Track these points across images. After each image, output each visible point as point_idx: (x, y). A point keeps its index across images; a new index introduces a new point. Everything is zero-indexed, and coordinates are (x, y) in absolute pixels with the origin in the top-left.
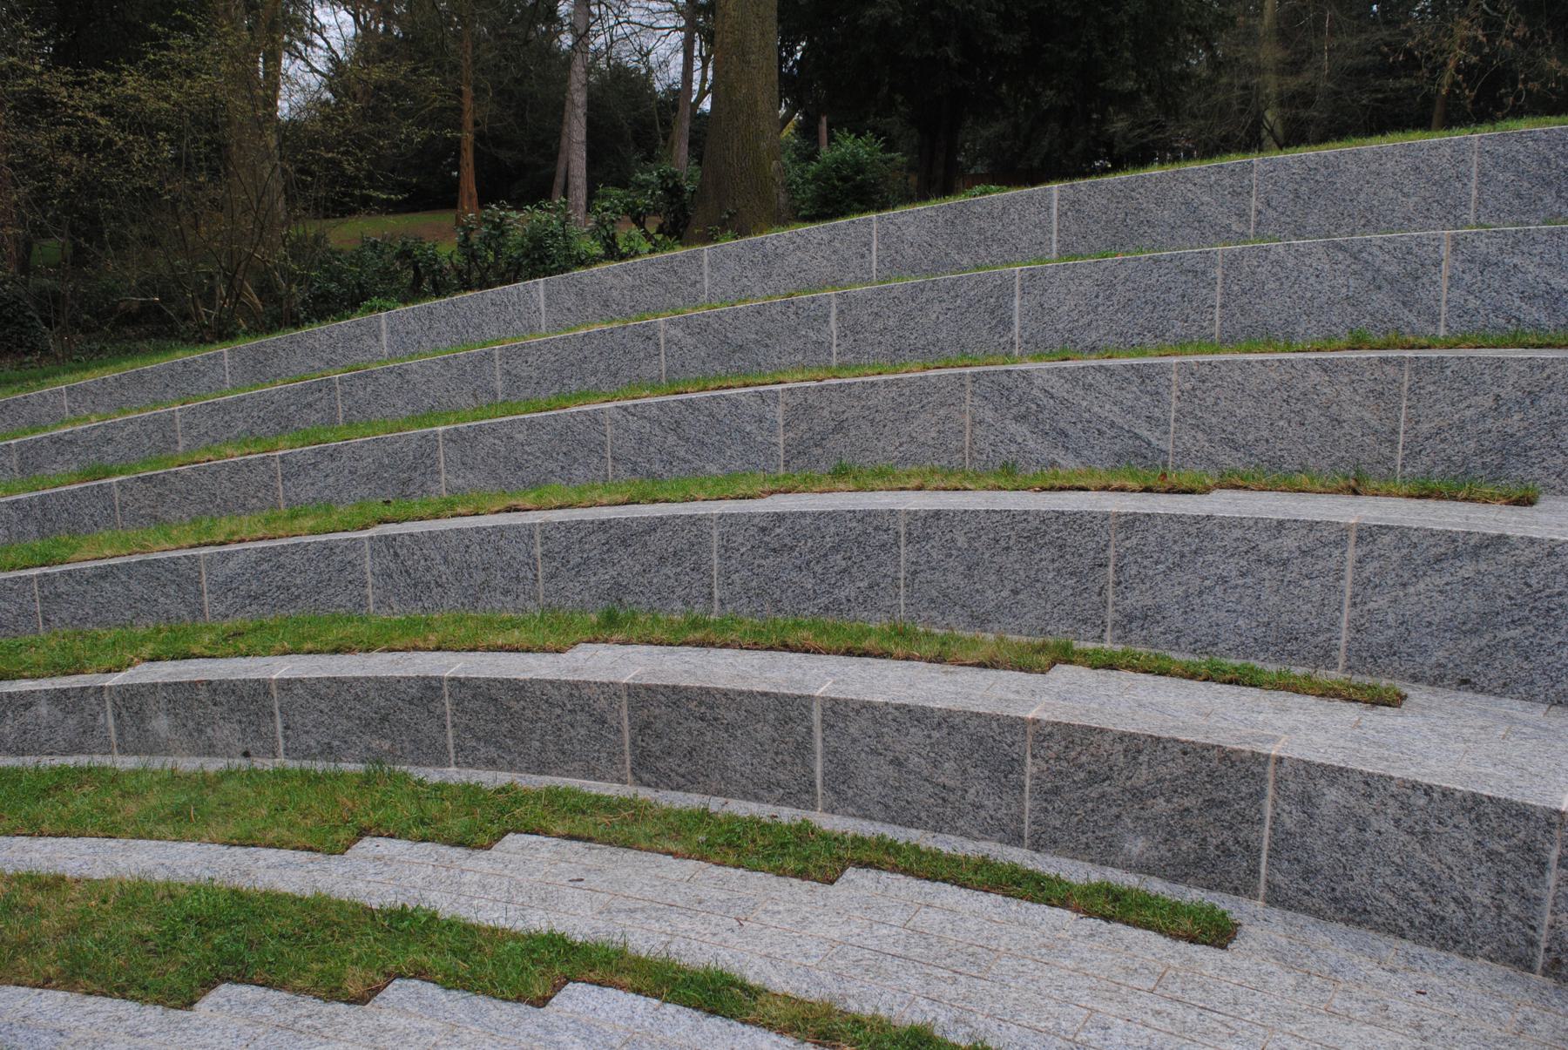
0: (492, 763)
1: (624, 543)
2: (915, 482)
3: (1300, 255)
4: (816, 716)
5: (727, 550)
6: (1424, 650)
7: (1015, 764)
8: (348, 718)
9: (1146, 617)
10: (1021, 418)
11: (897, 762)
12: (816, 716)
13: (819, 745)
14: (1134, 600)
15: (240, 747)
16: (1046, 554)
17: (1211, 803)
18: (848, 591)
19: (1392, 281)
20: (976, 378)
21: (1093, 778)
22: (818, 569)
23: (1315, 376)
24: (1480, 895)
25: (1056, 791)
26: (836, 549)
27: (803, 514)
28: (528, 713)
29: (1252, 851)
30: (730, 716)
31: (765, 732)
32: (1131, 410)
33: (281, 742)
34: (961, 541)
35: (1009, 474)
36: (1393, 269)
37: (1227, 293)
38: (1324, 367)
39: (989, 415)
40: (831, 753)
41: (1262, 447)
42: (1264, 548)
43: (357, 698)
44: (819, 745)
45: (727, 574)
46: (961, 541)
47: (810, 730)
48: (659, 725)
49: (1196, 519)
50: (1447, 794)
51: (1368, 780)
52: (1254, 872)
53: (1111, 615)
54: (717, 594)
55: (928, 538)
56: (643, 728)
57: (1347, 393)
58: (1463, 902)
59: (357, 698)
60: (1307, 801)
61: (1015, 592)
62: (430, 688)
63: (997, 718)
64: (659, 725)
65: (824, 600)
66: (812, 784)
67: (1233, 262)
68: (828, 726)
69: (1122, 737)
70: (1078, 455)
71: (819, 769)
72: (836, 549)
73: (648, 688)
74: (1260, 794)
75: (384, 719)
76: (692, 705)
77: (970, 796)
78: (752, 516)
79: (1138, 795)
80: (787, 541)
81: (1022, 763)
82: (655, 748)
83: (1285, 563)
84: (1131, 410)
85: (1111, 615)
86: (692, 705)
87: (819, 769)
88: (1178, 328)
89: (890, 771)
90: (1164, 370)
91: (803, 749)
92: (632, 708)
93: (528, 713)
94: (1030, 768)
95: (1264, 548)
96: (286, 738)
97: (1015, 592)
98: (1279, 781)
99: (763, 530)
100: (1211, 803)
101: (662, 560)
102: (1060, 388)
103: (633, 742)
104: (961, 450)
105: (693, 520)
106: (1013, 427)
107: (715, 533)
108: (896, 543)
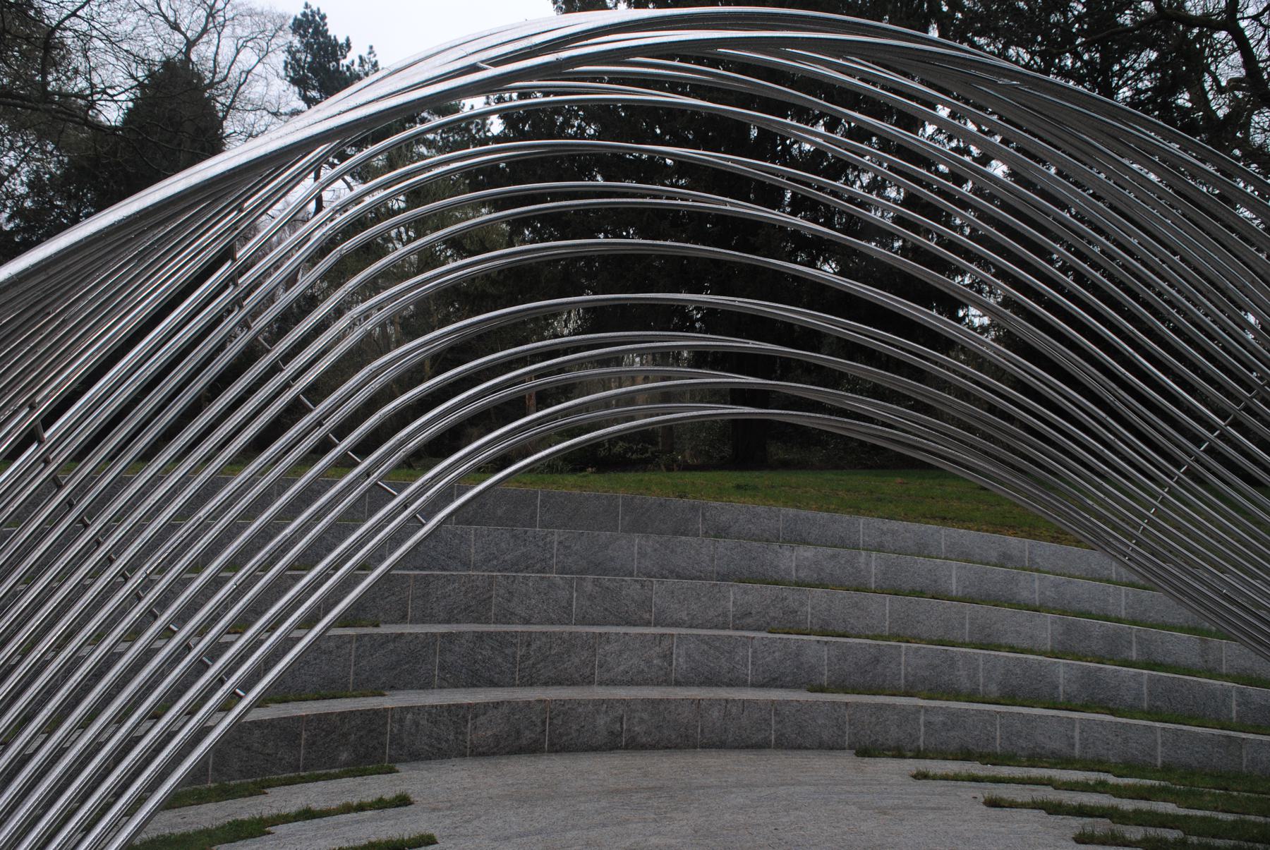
6: (378, 678)
11: (248, 749)
17: (370, 731)
24: (451, 737)
25: (314, 743)
29: (383, 745)
50: (441, 706)
51: (419, 708)
52: (384, 753)
58: (447, 741)
60: (401, 720)
63: (292, 718)
69: (340, 714)
74: (386, 723)
79: (345, 735)
81: (300, 734)
83: (331, 652)
94: (304, 735)
98: (393, 716)
100: (370, 731)
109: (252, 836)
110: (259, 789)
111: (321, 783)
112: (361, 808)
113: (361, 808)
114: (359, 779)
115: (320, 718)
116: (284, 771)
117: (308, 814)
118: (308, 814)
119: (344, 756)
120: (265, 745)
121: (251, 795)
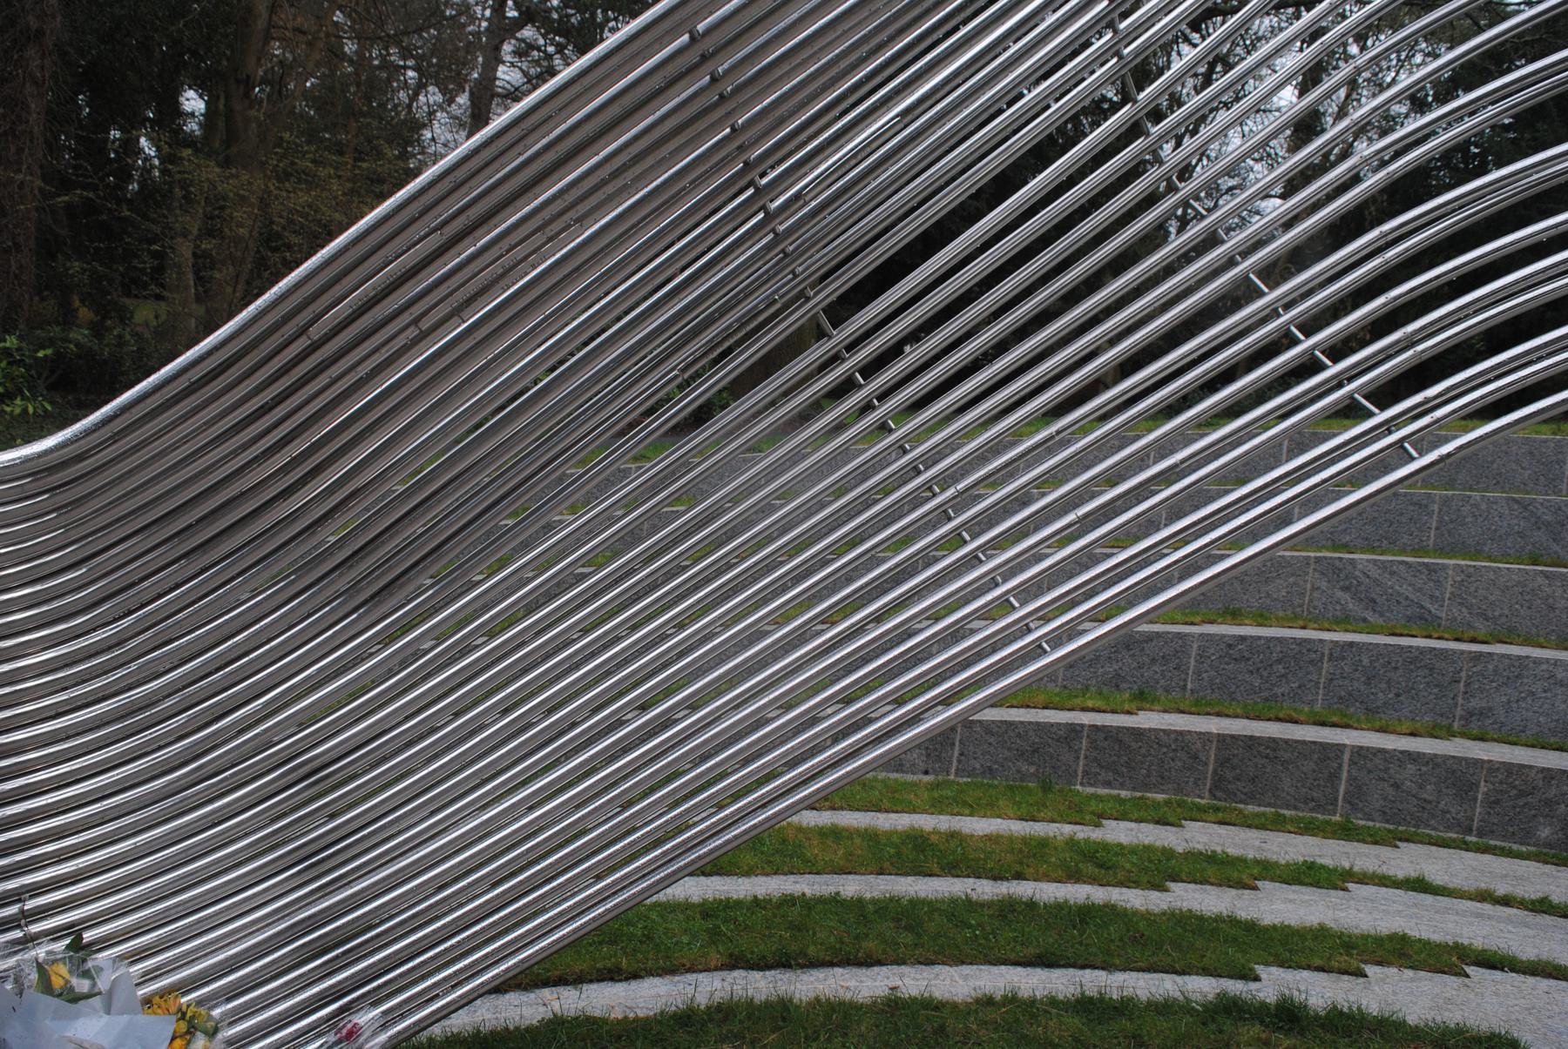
0: (1108, 784)
1: (1128, 648)
2: (1301, 623)
3: (1489, 502)
4: (1346, 757)
5: (1201, 657)
7: (1474, 786)
8: (1009, 749)
9: (1482, 714)
10: (1345, 589)
11: (1396, 786)
12: (1346, 757)
13: (1345, 775)
14: (1475, 703)
15: (922, 766)
16: (1421, 673)
18: (1284, 689)
19: (1548, 525)
20: (1318, 560)
21: (1522, 794)
22: (1265, 674)
23: (1540, 580)
25: (1497, 802)
26: (1279, 661)
27: (1260, 638)
28: (1143, 751)
30: (1286, 756)
31: (1308, 766)
32: (1420, 590)
33: (955, 763)
34: (1366, 662)
35: (1344, 621)
36: (1548, 518)
37: (1440, 521)
38: (1545, 575)
39: (1324, 585)
40: (1351, 779)
41: (1503, 620)
42: (1559, 676)
43: (1019, 735)
44: (1345, 775)
45: (1198, 673)
46: (1366, 662)
47: (1340, 766)
48: (1235, 761)
49: (1519, 658)
53: (1459, 712)
54: (1189, 686)
55: (1344, 658)
56: (1223, 762)
57: (1559, 592)
59: (1019, 735)
61: (1398, 695)
62: (1074, 730)
63: (1466, 759)
64: (1235, 761)
65: (1266, 694)
66: (1336, 799)
67: (1446, 501)
68: (1352, 762)
70: (1381, 615)
71: (1342, 789)
72: (1279, 661)
73: (1232, 736)
75: (1034, 751)
76: (1261, 748)
77: (1442, 806)
78: (1224, 636)
79: (1548, 803)
80: (1246, 654)
81: (1478, 785)
82: (1229, 775)
84: (1420, 590)
85: (1459, 712)
86: (1261, 748)
87: (1342, 789)
88: (1405, 539)
89: (1391, 791)
90: (1444, 567)
91: (1334, 777)
92: (1218, 749)
93: (1143, 751)
94: (1483, 788)
95: (1559, 676)
96: (959, 761)
97: (1398, 695)
99: (1230, 646)
101: (1153, 660)
102: (1375, 573)
103: (1215, 771)
104: (1301, 606)
105: (1180, 636)
106: (1339, 594)
107: (1195, 646)
108: (1321, 660)
109: (1316, 884)
110: (1391, 840)
111: (1487, 857)
112: (1506, 901)
113: (1506, 901)
114: (1549, 868)
115: (1510, 769)
116: (1449, 828)
117: (1419, 885)
118: (1419, 885)
119: (1545, 833)
120: (1421, 787)
121: (1376, 843)
